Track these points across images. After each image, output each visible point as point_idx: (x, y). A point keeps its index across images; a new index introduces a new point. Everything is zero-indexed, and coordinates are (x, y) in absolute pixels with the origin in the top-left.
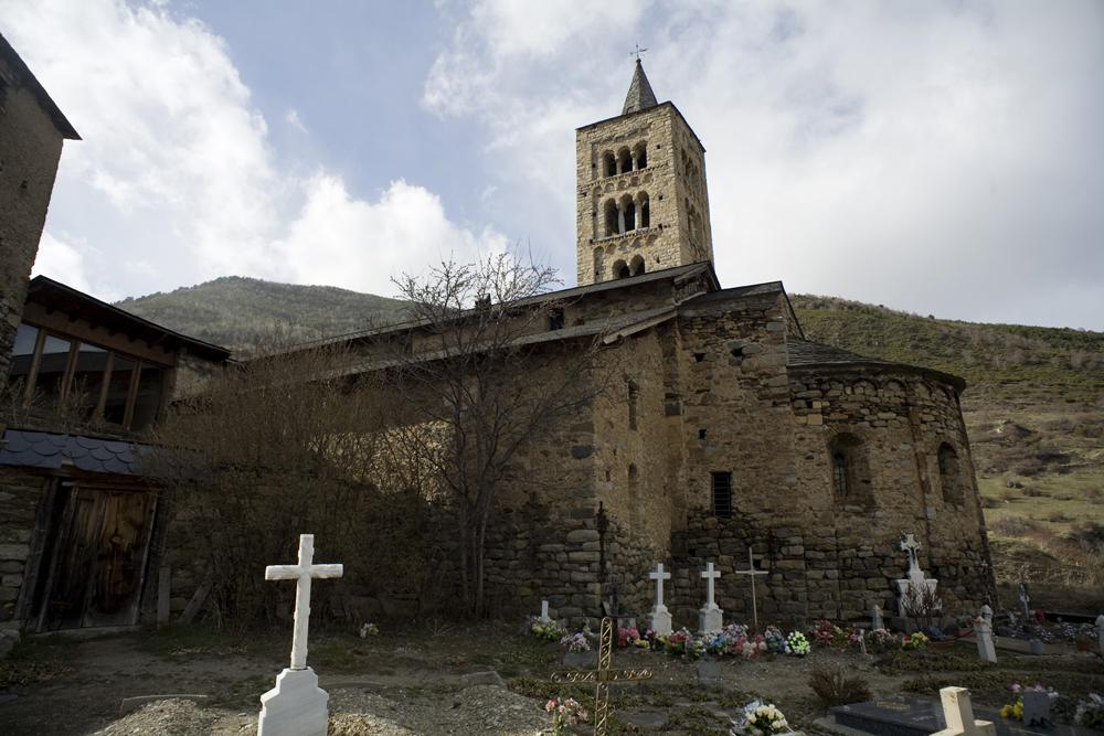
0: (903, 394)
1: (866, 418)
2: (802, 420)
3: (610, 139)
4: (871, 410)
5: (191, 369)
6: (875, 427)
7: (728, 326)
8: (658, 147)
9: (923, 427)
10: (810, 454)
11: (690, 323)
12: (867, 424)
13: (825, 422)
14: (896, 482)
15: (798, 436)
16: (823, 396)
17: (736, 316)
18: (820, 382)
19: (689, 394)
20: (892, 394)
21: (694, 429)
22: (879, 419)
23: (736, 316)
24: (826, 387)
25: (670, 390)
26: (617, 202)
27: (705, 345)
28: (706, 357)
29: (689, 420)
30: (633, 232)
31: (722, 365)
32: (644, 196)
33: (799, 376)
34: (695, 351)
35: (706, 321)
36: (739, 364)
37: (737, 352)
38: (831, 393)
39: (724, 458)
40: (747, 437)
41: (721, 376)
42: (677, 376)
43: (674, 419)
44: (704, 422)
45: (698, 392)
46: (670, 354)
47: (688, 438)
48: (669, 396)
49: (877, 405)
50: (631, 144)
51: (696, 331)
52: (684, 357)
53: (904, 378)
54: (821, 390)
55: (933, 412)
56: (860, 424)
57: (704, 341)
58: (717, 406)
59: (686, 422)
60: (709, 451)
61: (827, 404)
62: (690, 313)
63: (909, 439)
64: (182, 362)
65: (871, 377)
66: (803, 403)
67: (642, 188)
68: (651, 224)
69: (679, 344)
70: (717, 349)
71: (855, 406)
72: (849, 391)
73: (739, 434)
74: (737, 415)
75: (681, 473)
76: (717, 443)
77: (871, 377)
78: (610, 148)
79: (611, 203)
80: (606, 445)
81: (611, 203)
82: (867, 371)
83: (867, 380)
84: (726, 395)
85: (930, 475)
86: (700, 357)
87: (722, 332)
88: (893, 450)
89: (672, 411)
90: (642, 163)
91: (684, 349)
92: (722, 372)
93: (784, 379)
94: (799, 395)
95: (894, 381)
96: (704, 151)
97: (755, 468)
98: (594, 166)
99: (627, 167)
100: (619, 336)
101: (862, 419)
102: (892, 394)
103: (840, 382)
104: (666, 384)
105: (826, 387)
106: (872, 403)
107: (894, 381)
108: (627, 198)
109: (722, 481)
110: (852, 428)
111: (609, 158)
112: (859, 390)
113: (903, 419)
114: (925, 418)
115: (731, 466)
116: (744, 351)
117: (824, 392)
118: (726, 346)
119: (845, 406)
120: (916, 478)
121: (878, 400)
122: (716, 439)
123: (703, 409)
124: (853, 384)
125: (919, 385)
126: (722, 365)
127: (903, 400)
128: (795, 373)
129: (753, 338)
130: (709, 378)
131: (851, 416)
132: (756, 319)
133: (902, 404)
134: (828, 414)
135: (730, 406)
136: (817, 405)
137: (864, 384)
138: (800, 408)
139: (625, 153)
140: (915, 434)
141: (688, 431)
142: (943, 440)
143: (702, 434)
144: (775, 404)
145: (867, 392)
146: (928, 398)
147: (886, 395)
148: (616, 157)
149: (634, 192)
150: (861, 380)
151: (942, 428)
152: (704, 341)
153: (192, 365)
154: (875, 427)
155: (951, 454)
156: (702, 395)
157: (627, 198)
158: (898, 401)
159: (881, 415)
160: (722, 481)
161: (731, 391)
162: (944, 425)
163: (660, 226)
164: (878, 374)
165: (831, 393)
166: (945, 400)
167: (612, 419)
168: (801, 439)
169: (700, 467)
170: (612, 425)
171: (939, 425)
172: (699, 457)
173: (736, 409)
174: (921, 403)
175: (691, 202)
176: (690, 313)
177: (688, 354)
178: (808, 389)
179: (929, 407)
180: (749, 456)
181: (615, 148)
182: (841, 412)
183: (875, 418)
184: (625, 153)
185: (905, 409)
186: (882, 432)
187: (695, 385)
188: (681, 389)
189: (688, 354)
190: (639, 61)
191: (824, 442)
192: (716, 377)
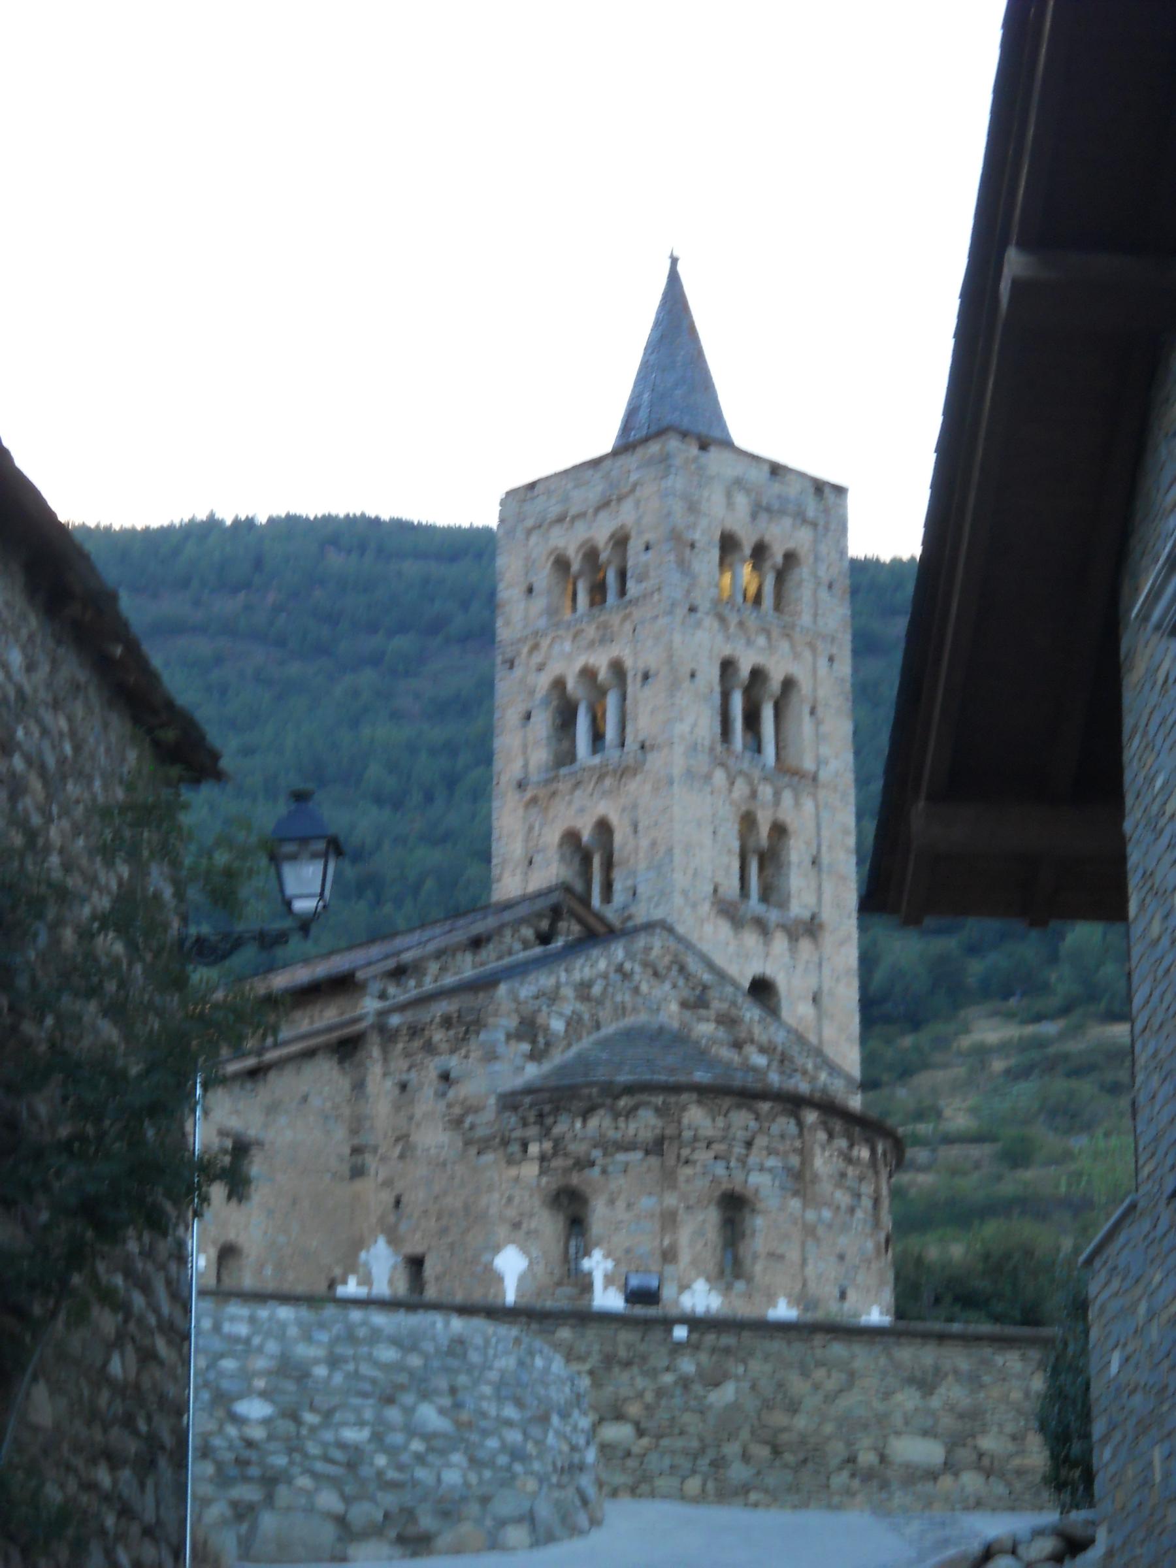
2: (513, 1172)
3: (560, 519)
7: (438, 1036)
9: (688, 1171)
11: (388, 1036)
13: (542, 1172)
16: (546, 1133)
17: (447, 1022)
18: (541, 1116)
21: (387, 1197)
23: (447, 1022)
25: (356, 1141)
26: (571, 685)
27: (410, 1069)
31: (426, 1101)
32: (618, 668)
33: (515, 1108)
35: (415, 1031)
36: (444, 1094)
37: (445, 1077)
39: (418, 1236)
43: (359, 1185)
45: (398, 1140)
46: (359, 1086)
48: (356, 1151)
50: (601, 532)
56: (587, 1172)
60: (403, 1228)
62: (395, 1020)
66: (515, 1148)
67: (614, 651)
72: (578, 1125)
78: (561, 543)
79: (559, 684)
81: (559, 684)
87: (430, 1048)
89: (358, 1172)
93: (489, 1115)
95: (648, 1103)
96: (840, 491)
101: (592, 1164)
102: (645, 1124)
104: (354, 1131)
108: (588, 674)
109: (416, 1264)
110: (575, 1179)
111: (561, 564)
112: (593, 1122)
116: (452, 1075)
118: (433, 1067)
124: (586, 1115)
126: (426, 1101)
128: (510, 1102)
129: (463, 1052)
136: (534, 1149)
139: (591, 555)
140: (668, 1179)
142: (725, 1186)
143: (398, 1203)
146: (708, 1122)
148: (575, 567)
149: (601, 661)
157: (588, 674)
160: (416, 1264)
161: (434, 1138)
164: (617, 1097)
176: (395, 1020)
177: (389, 1084)
180: (444, 1231)
184: (591, 555)
185: (656, 1147)
186: (618, 1182)
190: (674, 261)
191: (537, 1202)
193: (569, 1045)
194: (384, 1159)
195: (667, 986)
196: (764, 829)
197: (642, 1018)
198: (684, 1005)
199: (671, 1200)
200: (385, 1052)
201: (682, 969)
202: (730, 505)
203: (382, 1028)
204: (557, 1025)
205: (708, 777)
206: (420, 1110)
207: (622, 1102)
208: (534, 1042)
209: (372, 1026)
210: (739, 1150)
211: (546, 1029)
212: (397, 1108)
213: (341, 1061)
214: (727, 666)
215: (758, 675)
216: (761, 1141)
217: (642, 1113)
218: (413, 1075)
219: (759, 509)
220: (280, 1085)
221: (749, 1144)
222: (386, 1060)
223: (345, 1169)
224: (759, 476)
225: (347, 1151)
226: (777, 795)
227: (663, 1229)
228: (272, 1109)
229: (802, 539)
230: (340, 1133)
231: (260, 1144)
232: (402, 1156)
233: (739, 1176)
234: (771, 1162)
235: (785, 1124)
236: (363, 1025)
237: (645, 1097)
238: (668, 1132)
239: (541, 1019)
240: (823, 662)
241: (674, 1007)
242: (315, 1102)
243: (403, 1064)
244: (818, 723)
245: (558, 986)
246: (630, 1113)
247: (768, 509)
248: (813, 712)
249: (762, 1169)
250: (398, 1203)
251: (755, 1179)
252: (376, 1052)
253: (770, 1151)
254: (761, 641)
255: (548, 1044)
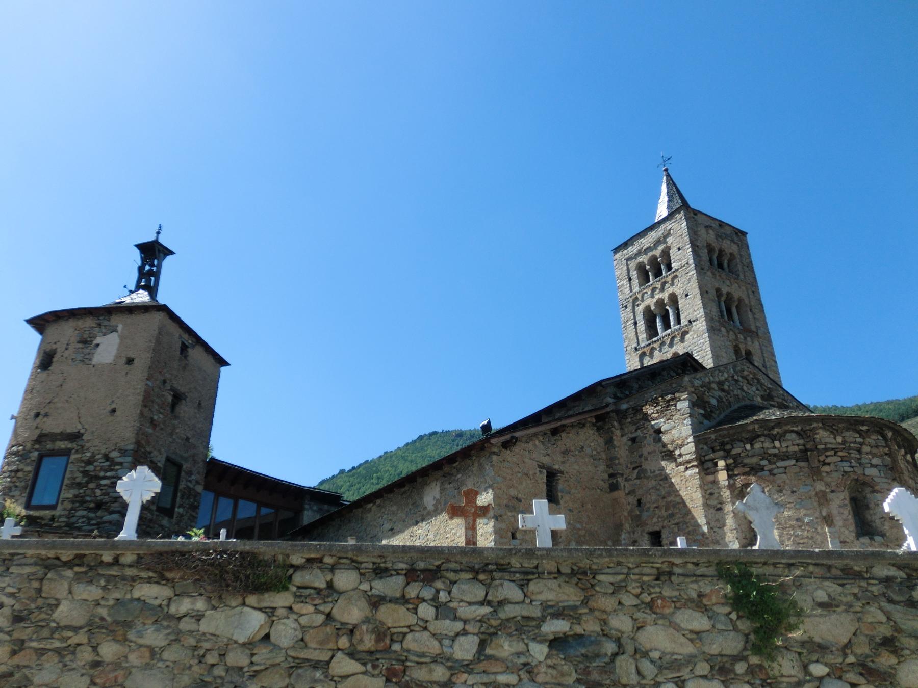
0: (801, 442)
1: (766, 468)
4: (769, 461)
5: (314, 511)
6: (774, 475)
8: (679, 249)
10: (719, 506)
12: (767, 473)
14: (797, 520)
15: (708, 492)
18: (723, 444)
19: (627, 471)
20: (790, 443)
21: (632, 500)
22: (778, 467)
24: (728, 447)
25: (611, 471)
26: (653, 308)
28: (637, 440)
29: (629, 493)
30: (669, 331)
34: (630, 436)
38: (734, 452)
39: (655, 520)
40: (669, 499)
41: (649, 453)
42: (616, 458)
43: (616, 494)
44: (639, 492)
45: (634, 469)
46: (609, 442)
47: (629, 507)
48: (611, 476)
49: (775, 455)
50: (657, 252)
51: (629, 420)
52: (621, 442)
53: (800, 428)
54: (724, 450)
55: (840, 454)
57: (635, 427)
58: (647, 478)
59: (627, 494)
60: (645, 515)
61: (731, 461)
63: (809, 481)
64: (307, 506)
65: (766, 432)
66: (710, 464)
67: (670, 290)
68: (682, 321)
69: (618, 433)
70: (645, 431)
71: (754, 460)
72: (748, 447)
73: (664, 498)
74: (661, 482)
75: (623, 536)
76: (649, 508)
77: (766, 432)
79: (648, 309)
80: (510, 514)
81: (648, 309)
82: (761, 427)
83: (763, 435)
84: (652, 469)
85: (835, 512)
86: (633, 440)
88: (793, 492)
89: (614, 487)
90: (669, 267)
91: (622, 436)
92: (650, 449)
94: (707, 458)
95: (792, 431)
96: (744, 234)
97: (677, 524)
98: (630, 280)
99: (658, 273)
100: (512, 437)
101: (763, 470)
102: (792, 444)
103: (741, 441)
105: (728, 447)
106: (770, 455)
107: (792, 431)
108: (660, 303)
111: (641, 268)
112: (757, 446)
113: (802, 464)
114: (828, 460)
115: (661, 524)
117: (730, 451)
119: (747, 461)
120: (817, 514)
121: (776, 451)
122: (648, 505)
123: (638, 481)
124: (751, 441)
125: (821, 431)
127: (801, 447)
130: (641, 456)
131: (752, 469)
132: (668, 401)
133: (801, 451)
134: (733, 470)
135: (656, 476)
137: (762, 439)
138: (708, 468)
141: (626, 501)
143: (639, 501)
144: (687, 469)
145: (766, 445)
146: (833, 441)
147: (784, 445)
148: (648, 267)
150: (759, 436)
151: (852, 467)
152: (635, 427)
153: (315, 508)
154: (774, 475)
155: (868, 489)
156: (636, 471)
158: (796, 448)
159: (780, 464)
162: (854, 463)
163: (690, 322)
164: (773, 428)
165: (734, 452)
166: (860, 440)
167: (520, 496)
168: (711, 494)
169: (639, 529)
170: (520, 500)
171: (845, 464)
172: (637, 521)
173: (659, 478)
174: (823, 447)
175: (725, 290)
178: (714, 451)
179: (833, 449)
180: (672, 516)
181: (644, 259)
182: (743, 466)
183: (774, 466)
185: (803, 456)
187: (631, 463)
188: (619, 469)
189: (625, 439)
192: (645, 452)
193: (720, 413)
194: (626, 480)
195: (754, 389)
196: (743, 353)
197: (748, 402)
198: (762, 397)
199: (820, 486)
200: (620, 422)
201: (759, 381)
202: (708, 233)
203: (617, 412)
204: (714, 402)
205: (720, 330)
206: (645, 451)
207: (775, 431)
208: (705, 410)
209: (612, 411)
210: (854, 454)
211: (709, 403)
212: (631, 451)
213: (598, 429)
214: (718, 291)
215: (728, 294)
216: (866, 449)
217: (789, 436)
218: (639, 433)
219: (718, 236)
220: (568, 440)
221: (859, 451)
222: (622, 429)
223: (607, 485)
224: (715, 225)
225: (606, 476)
226: (745, 339)
227: (820, 504)
228: (565, 452)
229: (734, 248)
230: (602, 467)
231: (562, 473)
232: (638, 478)
233: (859, 471)
234: (875, 461)
235: (874, 438)
236: (608, 409)
237: (789, 427)
238: (808, 446)
239: (706, 399)
240: (750, 293)
241: (759, 399)
242: (588, 450)
243: (633, 428)
244: (754, 314)
245: (709, 383)
246: (781, 437)
247: (721, 237)
248: (751, 310)
249: (872, 466)
250: (639, 501)
251: (871, 472)
252: (615, 423)
253: (874, 455)
254: (728, 283)
255: (711, 411)
